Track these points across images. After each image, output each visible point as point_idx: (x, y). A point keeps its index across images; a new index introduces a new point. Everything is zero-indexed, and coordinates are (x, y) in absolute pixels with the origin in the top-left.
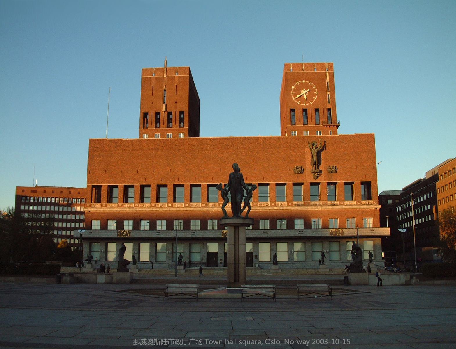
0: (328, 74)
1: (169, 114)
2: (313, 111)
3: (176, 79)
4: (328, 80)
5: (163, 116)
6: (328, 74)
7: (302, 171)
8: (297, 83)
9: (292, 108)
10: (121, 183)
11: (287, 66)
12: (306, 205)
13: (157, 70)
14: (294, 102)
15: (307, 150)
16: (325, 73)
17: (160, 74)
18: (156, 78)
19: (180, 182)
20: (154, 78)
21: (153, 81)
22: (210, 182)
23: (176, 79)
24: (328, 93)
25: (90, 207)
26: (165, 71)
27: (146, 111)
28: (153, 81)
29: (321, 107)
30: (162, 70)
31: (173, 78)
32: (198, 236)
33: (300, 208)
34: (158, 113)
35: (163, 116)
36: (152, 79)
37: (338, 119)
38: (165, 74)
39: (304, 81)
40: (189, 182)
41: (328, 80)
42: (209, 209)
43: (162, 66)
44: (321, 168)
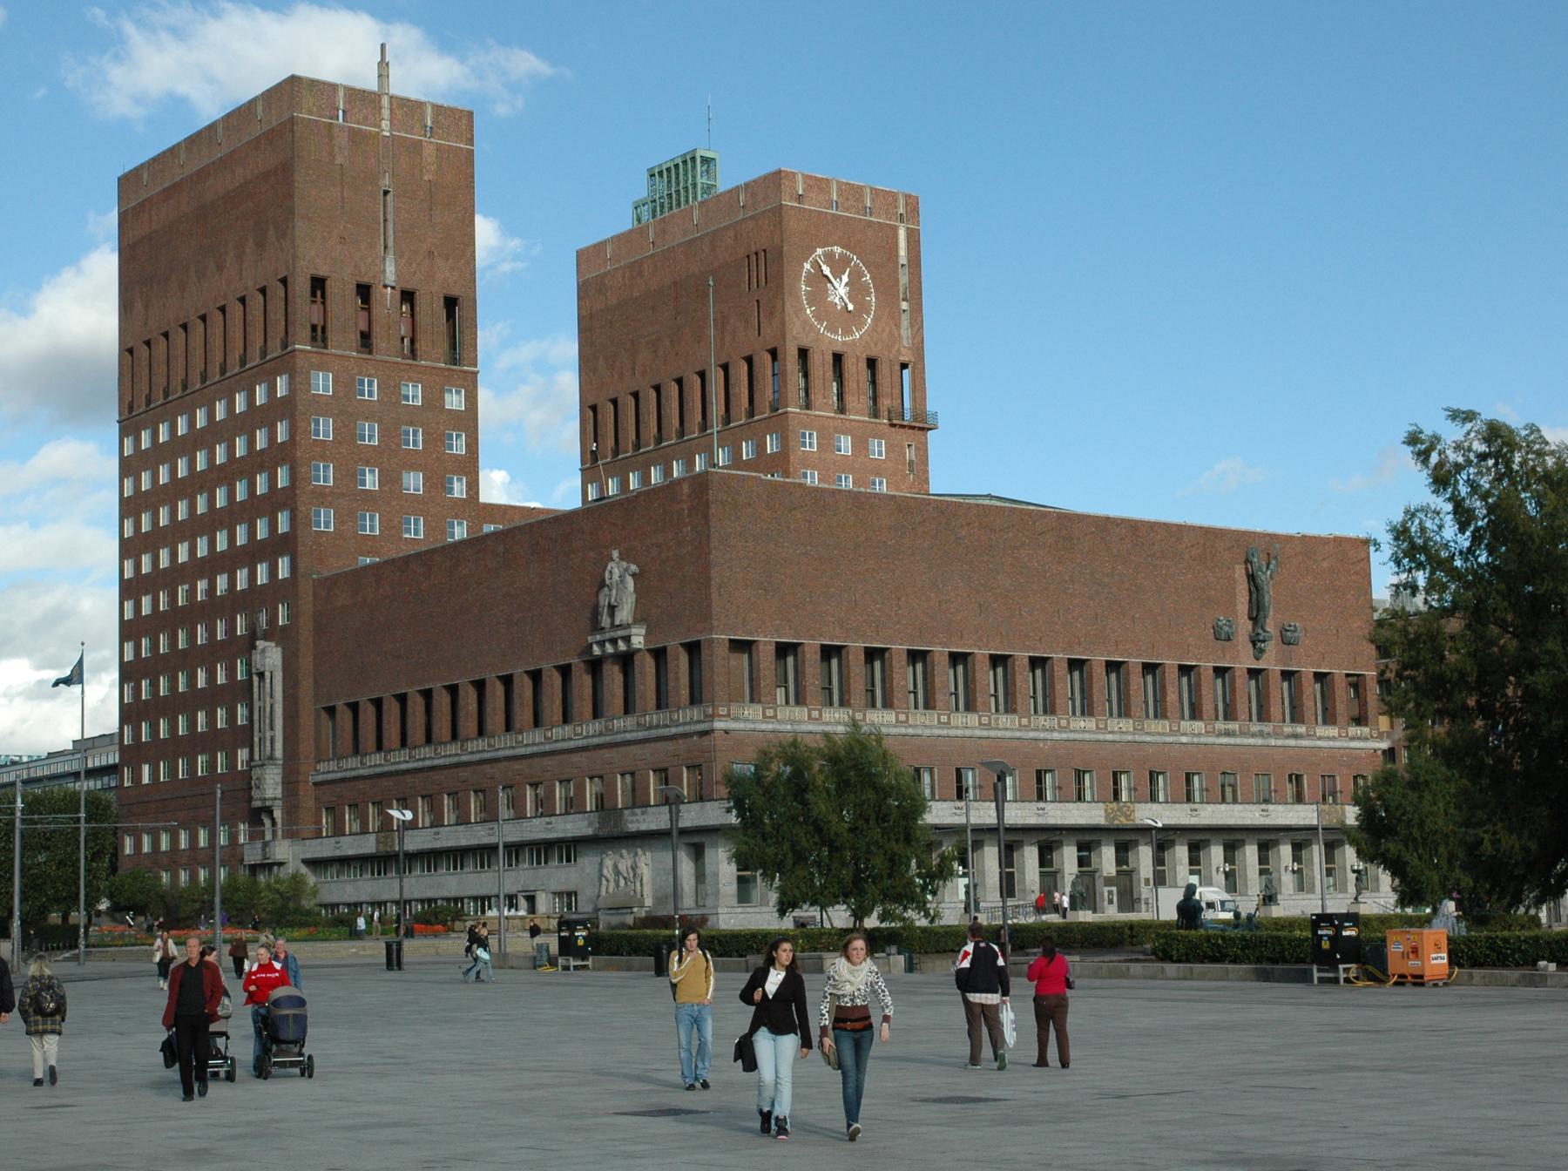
0: (902, 234)
1: (408, 296)
2: (863, 365)
4: (903, 259)
6: (902, 234)
8: (819, 251)
9: (805, 343)
10: (812, 637)
12: (1243, 734)
13: (357, 96)
14: (806, 321)
15: (1240, 572)
16: (895, 229)
17: (366, 118)
18: (352, 131)
19: (964, 645)
20: (342, 128)
21: (342, 140)
22: (1034, 650)
23: (429, 154)
24: (904, 305)
25: (728, 715)
26: (386, 113)
27: (321, 273)
28: (342, 140)
31: (416, 147)
32: (1051, 821)
33: (1232, 741)
36: (336, 130)
37: (931, 406)
38: (385, 124)
39: (837, 250)
40: (986, 646)
41: (903, 259)
42: (1042, 735)
43: (371, 84)
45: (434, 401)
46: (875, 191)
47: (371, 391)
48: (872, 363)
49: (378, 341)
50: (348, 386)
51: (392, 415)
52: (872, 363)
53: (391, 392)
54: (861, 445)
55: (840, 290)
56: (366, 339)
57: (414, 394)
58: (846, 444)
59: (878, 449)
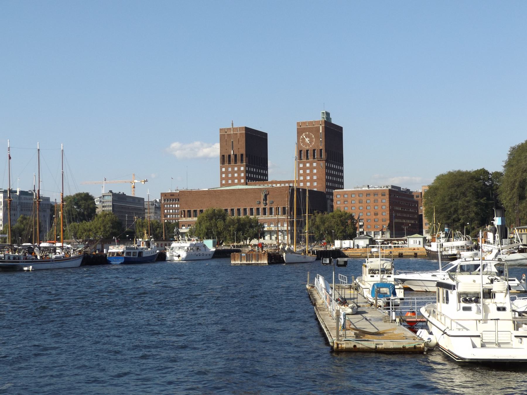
1: (236, 156)
3: (238, 135)
5: (232, 157)
7: (260, 203)
11: (298, 123)
13: (228, 129)
16: (319, 127)
21: (226, 136)
23: (238, 135)
28: (226, 136)
29: (317, 148)
30: (230, 129)
31: (236, 134)
34: (229, 156)
35: (232, 157)
44: (267, 202)
45: (239, 169)
46: (315, 122)
47: (230, 169)
48: (314, 150)
49: (231, 162)
50: (227, 170)
51: (233, 172)
52: (314, 150)
53: (233, 169)
54: (311, 164)
55: (307, 140)
56: (229, 162)
57: (236, 169)
58: (308, 165)
59: (315, 165)
